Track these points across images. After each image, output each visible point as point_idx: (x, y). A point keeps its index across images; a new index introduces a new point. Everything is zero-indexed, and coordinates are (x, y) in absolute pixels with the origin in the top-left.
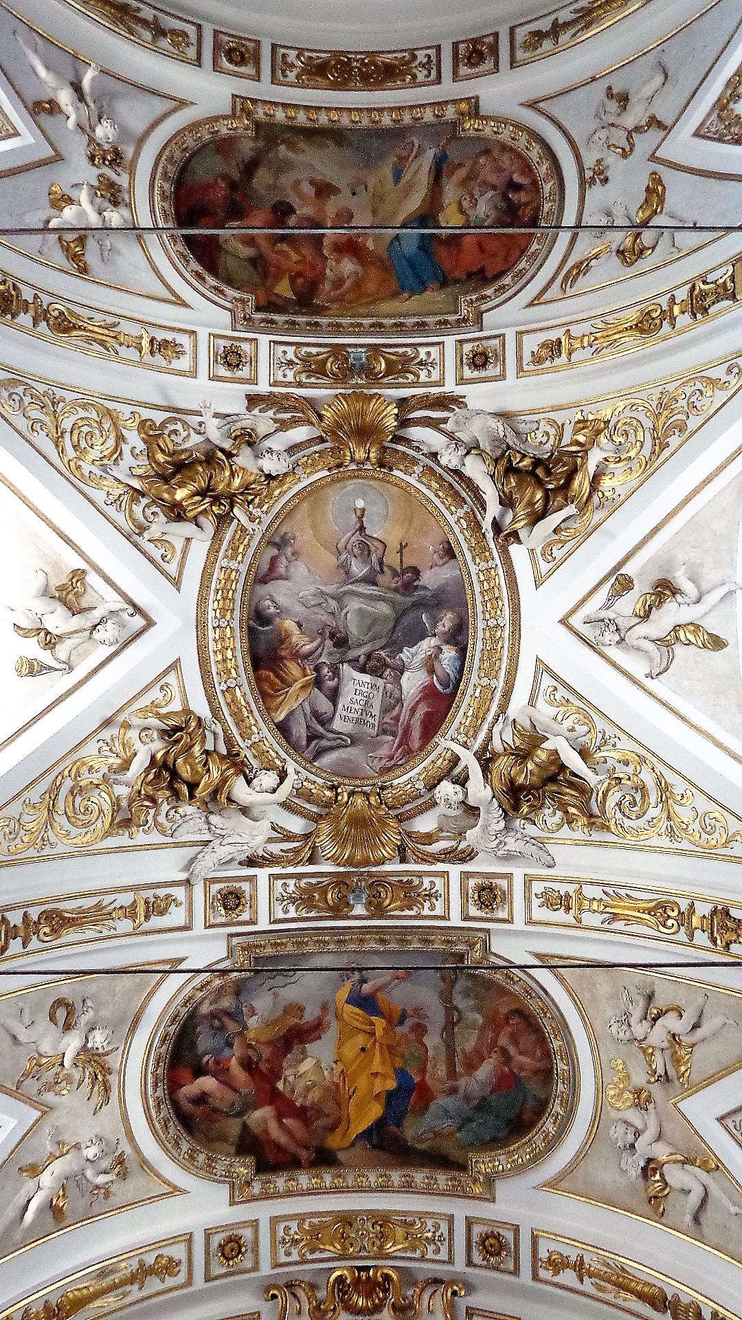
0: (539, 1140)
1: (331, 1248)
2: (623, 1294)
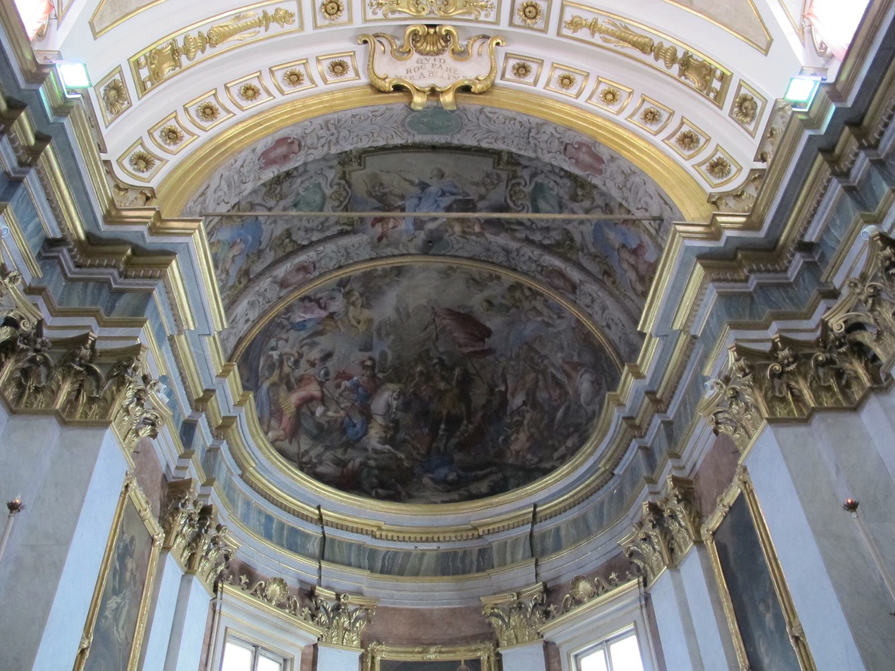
1: (407, 11)
2: (622, 43)
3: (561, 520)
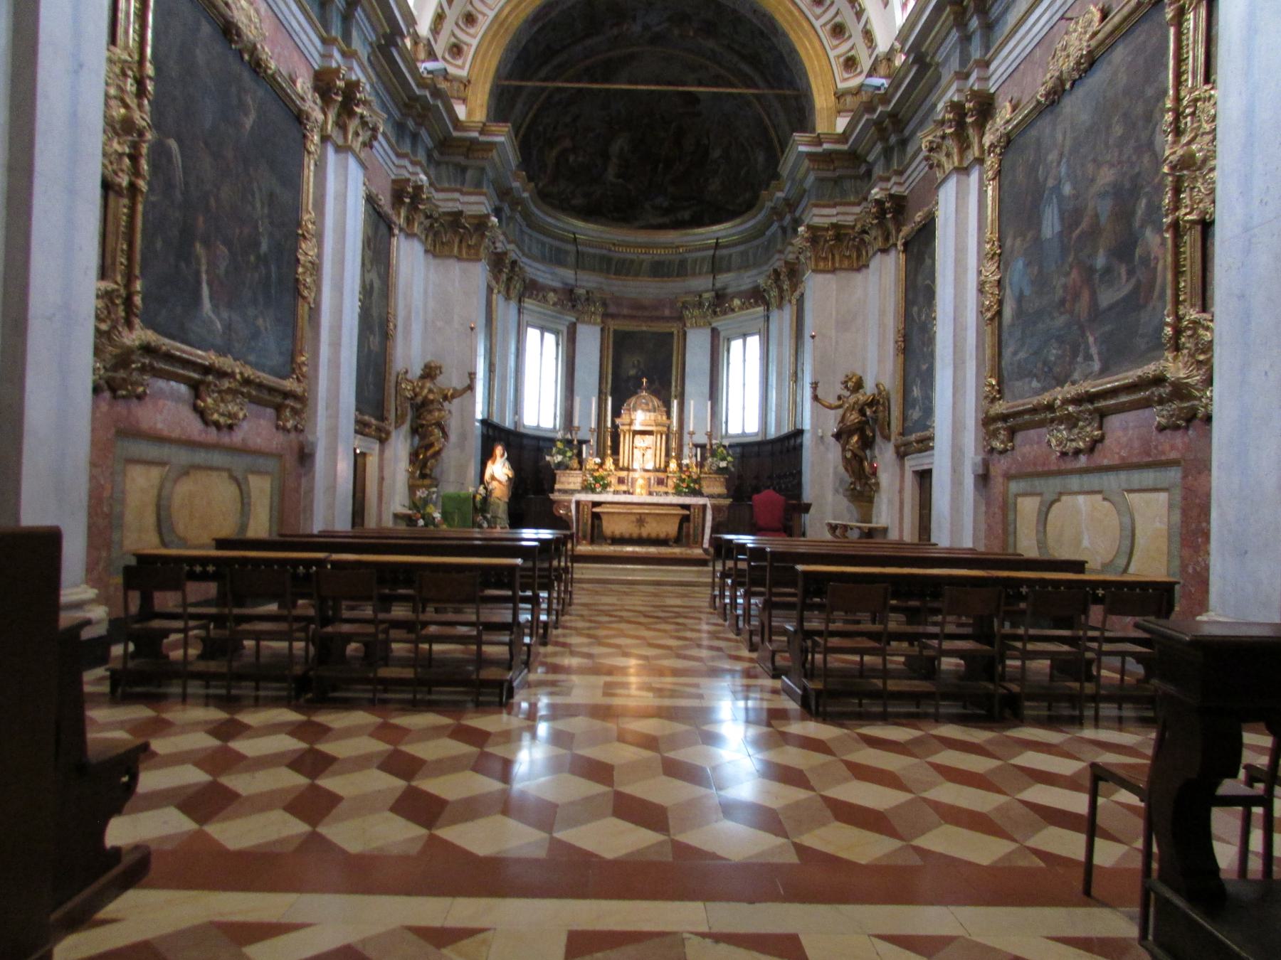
3: (733, 250)
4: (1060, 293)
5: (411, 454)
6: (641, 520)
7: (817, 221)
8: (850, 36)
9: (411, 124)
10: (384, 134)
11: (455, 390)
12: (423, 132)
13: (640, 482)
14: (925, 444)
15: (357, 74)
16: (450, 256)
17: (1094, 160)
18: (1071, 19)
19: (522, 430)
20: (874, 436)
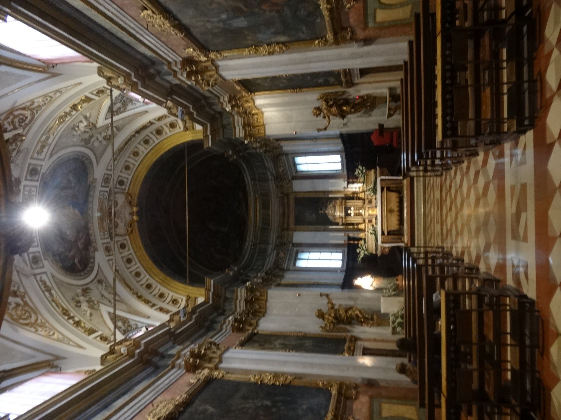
0: (88, 165)
4: (274, 13)
5: (362, 325)
6: (390, 211)
7: (242, 135)
8: (161, 127)
9: (207, 324)
10: (212, 338)
11: (329, 303)
12: (211, 317)
13: (370, 212)
14: (348, 73)
15: (187, 352)
16: (266, 304)
17: (210, 4)
18: (147, 25)
19: (345, 267)
20: (343, 99)
